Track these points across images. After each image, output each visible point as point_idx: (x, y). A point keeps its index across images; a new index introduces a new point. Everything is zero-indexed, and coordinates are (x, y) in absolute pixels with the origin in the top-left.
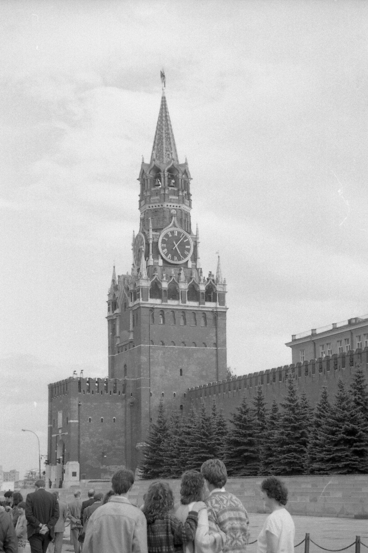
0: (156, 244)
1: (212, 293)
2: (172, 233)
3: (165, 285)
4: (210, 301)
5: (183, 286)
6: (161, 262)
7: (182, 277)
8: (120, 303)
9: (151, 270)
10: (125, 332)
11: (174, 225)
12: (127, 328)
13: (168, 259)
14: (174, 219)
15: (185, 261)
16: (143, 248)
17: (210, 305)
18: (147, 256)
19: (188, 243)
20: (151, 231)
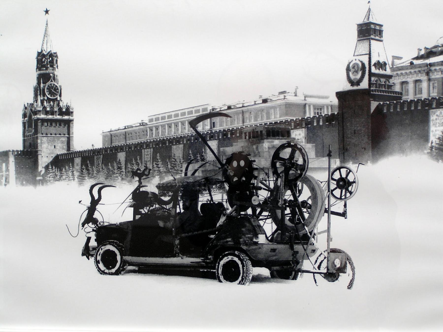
0: (44, 90)
1: (68, 112)
2: (51, 84)
3: (48, 109)
4: (67, 115)
5: (56, 109)
6: (46, 98)
7: (55, 105)
8: (28, 115)
9: (42, 102)
10: (30, 129)
11: (52, 81)
12: (32, 127)
13: (49, 96)
14: (52, 78)
15: (56, 97)
16: (38, 91)
17: (66, 117)
18: (40, 95)
19: (58, 89)
20: (42, 84)
